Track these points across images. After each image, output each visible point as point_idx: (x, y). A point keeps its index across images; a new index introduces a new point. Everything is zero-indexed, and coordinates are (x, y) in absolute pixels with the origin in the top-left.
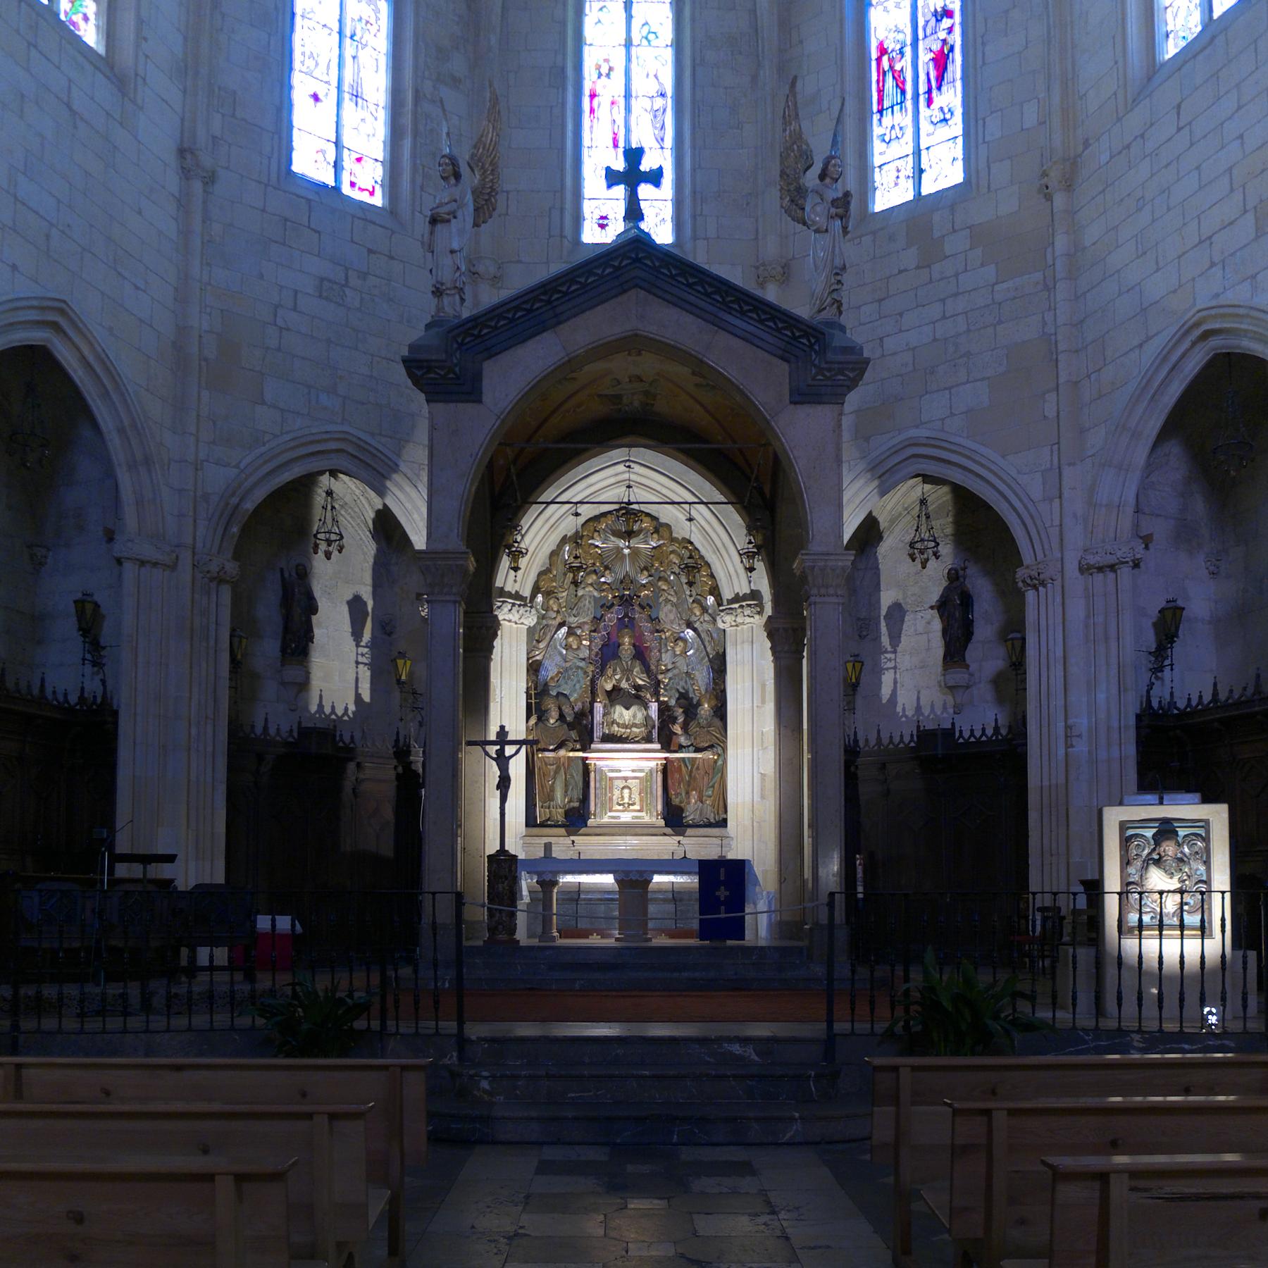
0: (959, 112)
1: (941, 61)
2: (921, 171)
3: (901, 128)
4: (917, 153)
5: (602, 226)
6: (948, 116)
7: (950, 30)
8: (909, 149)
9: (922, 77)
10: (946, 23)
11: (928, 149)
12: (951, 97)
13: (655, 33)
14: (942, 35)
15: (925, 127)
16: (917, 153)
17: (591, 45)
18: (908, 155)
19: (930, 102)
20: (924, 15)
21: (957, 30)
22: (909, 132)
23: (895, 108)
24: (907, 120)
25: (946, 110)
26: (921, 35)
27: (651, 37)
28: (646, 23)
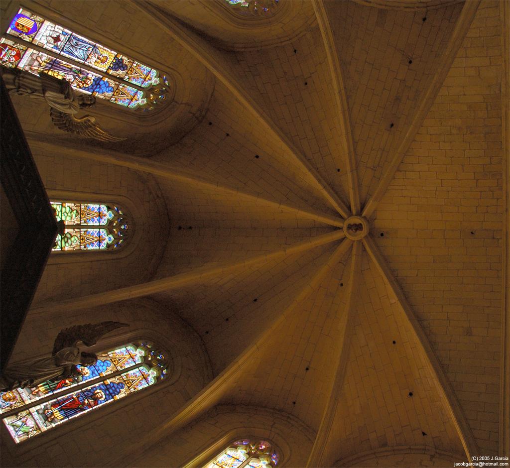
0: (54, 425)
1: (75, 406)
2: (16, 414)
3: (37, 392)
4: (27, 407)
6: (50, 420)
7: (89, 406)
8: (28, 402)
11: (30, 413)
12: (60, 418)
16: (27, 407)
18: (24, 402)
19: (54, 405)
20: (92, 388)
22: (38, 398)
23: (47, 386)
27: (66, 239)
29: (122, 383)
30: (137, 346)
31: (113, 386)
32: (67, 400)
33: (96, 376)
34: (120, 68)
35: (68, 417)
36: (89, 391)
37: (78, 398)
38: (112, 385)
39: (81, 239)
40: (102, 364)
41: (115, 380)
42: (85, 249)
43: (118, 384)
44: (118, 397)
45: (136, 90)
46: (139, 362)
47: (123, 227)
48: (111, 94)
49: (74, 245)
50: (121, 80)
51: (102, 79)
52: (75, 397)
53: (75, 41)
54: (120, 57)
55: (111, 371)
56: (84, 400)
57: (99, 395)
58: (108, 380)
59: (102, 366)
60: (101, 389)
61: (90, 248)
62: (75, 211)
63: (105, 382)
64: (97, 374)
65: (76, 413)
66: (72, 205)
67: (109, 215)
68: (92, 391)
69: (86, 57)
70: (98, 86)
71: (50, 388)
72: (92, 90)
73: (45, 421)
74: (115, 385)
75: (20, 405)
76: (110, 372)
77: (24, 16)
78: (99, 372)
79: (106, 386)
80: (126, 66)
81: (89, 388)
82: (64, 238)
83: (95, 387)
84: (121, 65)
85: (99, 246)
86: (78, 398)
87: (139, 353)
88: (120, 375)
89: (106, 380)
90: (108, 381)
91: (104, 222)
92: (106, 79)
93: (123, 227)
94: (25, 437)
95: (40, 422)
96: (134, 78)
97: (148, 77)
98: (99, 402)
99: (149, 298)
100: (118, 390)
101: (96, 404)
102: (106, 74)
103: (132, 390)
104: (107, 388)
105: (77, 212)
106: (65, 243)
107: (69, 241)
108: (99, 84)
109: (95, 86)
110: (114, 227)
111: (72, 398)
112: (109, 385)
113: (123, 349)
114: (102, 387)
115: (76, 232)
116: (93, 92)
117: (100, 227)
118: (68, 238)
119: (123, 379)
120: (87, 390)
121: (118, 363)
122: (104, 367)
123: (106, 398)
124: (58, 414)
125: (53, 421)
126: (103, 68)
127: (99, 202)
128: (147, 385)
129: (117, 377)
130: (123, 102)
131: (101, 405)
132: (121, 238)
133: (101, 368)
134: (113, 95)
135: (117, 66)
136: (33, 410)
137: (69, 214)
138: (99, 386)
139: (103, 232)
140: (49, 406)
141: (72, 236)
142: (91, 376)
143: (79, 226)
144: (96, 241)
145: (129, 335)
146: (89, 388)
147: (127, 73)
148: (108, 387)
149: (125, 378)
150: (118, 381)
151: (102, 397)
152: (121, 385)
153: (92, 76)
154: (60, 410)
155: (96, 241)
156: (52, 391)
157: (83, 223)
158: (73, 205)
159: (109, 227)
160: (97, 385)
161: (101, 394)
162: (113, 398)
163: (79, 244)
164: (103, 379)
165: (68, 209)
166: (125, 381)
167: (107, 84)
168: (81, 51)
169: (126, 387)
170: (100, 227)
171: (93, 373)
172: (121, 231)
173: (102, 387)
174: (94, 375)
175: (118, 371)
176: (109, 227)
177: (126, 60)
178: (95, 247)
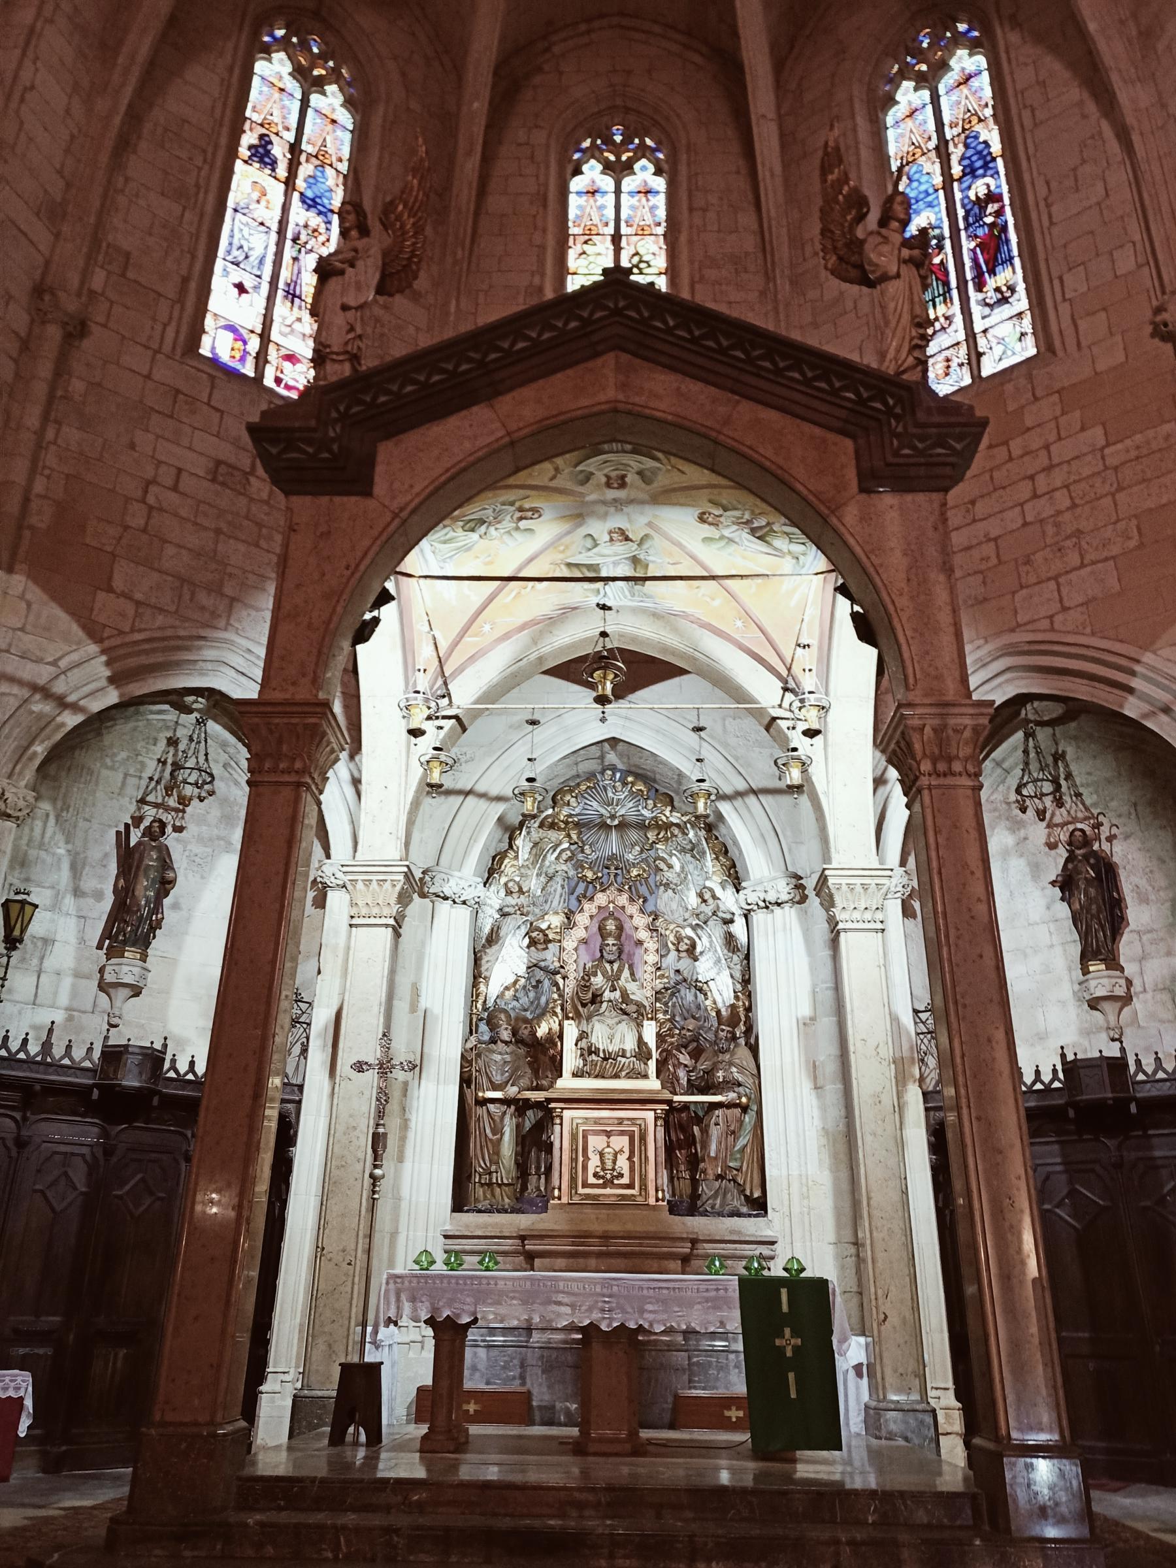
2: (980, 355)
4: (971, 336)
6: (1008, 294)
7: (999, 213)
8: (961, 336)
9: (968, 263)
10: (992, 208)
11: (985, 331)
12: (1012, 275)
13: (647, 262)
14: (989, 220)
15: (977, 310)
16: (971, 336)
17: (575, 274)
18: (958, 343)
19: (980, 287)
20: (963, 206)
21: (1008, 210)
23: (937, 300)
24: (956, 308)
25: (1004, 289)
26: (962, 225)
27: (642, 265)
28: (637, 254)
29: (967, 137)
30: (891, 101)
31: (969, 158)
32: (975, 260)
33: (937, 197)
34: (268, 153)
35: (1011, 258)
36: (967, 213)
37: (976, 236)
38: (966, 162)
39: (642, 232)
40: (915, 184)
41: (956, 152)
42: (664, 224)
43: (967, 146)
44: (996, 148)
45: (310, 112)
46: (925, 94)
47: (618, 138)
48: (330, 172)
49: (655, 249)
50: (295, 148)
51: (302, 194)
52: (973, 245)
53: (235, 253)
54: (244, 152)
55: (933, 163)
56: (985, 223)
57: (982, 192)
58: (953, 171)
59: (920, 183)
60: (969, 188)
61: (662, 213)
62: (586, 247)
63: (956, 177)
64: (934, 196)
65: (1008, 241)
66: (572, 254)
67: (592, 172)
68: (969, 207)
69: (262, 228)
70: (318, 200)
71: (944, 295)
72: (329, 214)
73: (1008, 302)
74: (968, 155)
75: (964, 347)
76: (937, 167)
77: (213, 349)
78: (931, 191)
79: (964, 175)
80: (262, 137)
81: (961, 213)
82: (640, 269)
83: (962, 200)
84: (261, 150)
85: (657, 192)
86: (976, 236)
87: (908, 95)
88: (947, 142)
89: (951, 175)
90: (956, 170)
91: (607, 183)
92: (300, 183)
93: (618, 138)
94: (1030, 340)
95: (1006, 311)
96: (284, 118)
97: (275, 81)
98: (998, 191)
99: (779, 67)
100: (981, 147)
101: (998, 198)
102: (289, 183)
103: (989, 112)
104: (970, 172)
105: (586, 242)
106: (649, 266)
107: (645, 259)
108: (313, 200)
109: (320, 207)
110: (618, 157)
111: (974, 251)
112: (965, 167)
113: (891, 134)
114: (965, 185)
115: (628, 244)
116: (332, 211)
117: (618, 191)
118: (641, 261)
119: (959, 135)
120: (966, 218)
121: (920, 147)
122: (924, 179)
123: (992, 176)
124: (1003, 276)
125: (1012, 289)
126: (277, 191)
127: (564, 193)
128: (986, 75)
129: (951, 148)
130: (341, 144)
131: (1005, 189)
132: (642, 142)
133: (923, 188)
134: (331, 165)
135: (267, 160)
136: (978, 327)
137: (591, 259)
138: (962, 191)
139: (628, 184)
140: (980, 296)
141: (637, 254)
142: (936, 209)
143: (616, 239)
144: (648, 200)
145: (861, 121)
146: (961, 213)
147: (277, 134)
148: (968, 170)
149: (956, 131)
150: (961, 146)
151: (988, 186)
152: (969, 139)
153: (299, 214)
154: (992, 272)
155: (648, 200)
156: (949, 290)
157: (610, 230)
158: (571, 252)
159: (619, 170)
160: (958, 196)
161: (979, 188)
162: (994, 159)
163: (653, 238)
164: (948, 180)
165: (582, 261)
166: (964, 130)
167: (311, 180)
168: (251, 239)
169: (978, 128)
170: (618, 191)
171: (930, 205)
172: (627, 140)
173: (965, 185)
174: (935, 202)
175: (937, 148)
176: (619, 170)
177: (249, 138)
178: (660, 201)
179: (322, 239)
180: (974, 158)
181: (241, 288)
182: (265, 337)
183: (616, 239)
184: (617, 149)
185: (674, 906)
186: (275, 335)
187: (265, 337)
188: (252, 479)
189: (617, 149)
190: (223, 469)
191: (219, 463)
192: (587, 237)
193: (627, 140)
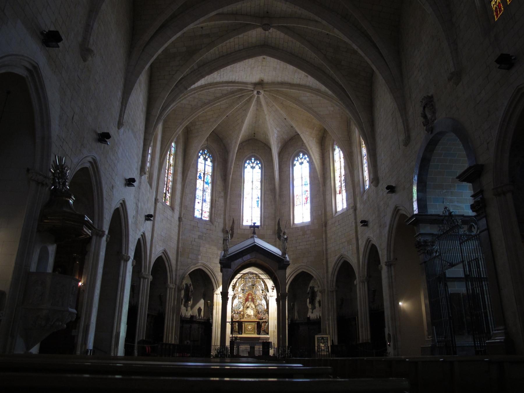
5: (247, 221)
10: (307, 192)
99: (280, 154)
132: (257, 162)
143: (252, 182)
172: (255, 161)
179: (208, 189)
180: (306, 182)
181: (198, 203)
182: (202, 210)
183: (252, 182)
184: (253, 163)
185: (259, 293)
186: (203, 209)
187: (202, 210)
188: (203, 237)
189: (253, 163)
190: (200, 236)
191: (199, 235)
192: (247, 182)
193: (255, 161)
